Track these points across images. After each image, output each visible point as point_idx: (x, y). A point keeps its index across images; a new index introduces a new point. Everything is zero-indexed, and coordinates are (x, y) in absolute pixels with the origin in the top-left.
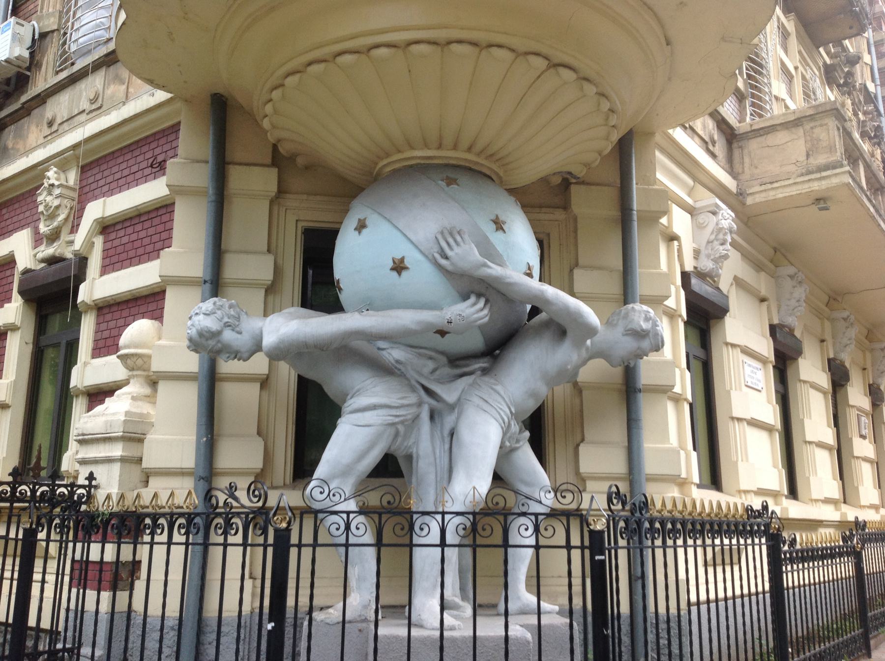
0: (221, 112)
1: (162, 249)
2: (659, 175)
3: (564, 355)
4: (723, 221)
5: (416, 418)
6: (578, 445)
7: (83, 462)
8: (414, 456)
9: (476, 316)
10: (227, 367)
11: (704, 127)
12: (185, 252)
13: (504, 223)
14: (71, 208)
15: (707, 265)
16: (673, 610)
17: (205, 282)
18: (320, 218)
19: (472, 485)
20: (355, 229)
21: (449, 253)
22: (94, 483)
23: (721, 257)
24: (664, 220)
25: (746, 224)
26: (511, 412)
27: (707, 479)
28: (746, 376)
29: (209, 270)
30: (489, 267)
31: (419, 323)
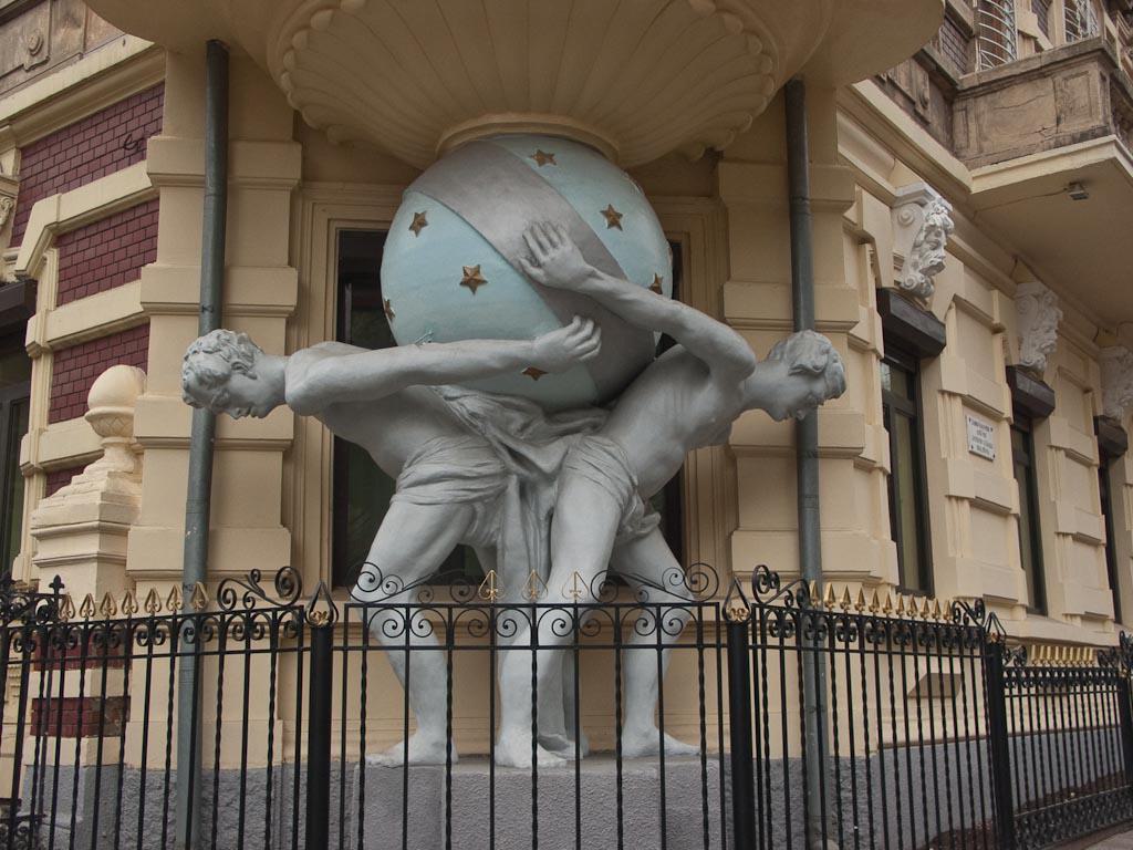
0: (223, 73)
1: (144, 265)
2: (841, 149)
3: (704, 400)
4: (935, 216)
5: (501, 494)
6: (731, 534)
7: (43, 565)
8: (499, 547)
9: (580, 347)
10: (237, 427)
11: (910, 81)
12: (175, 271)
13: (620, 216)
14: (11, 209)
15: (912, 277)
16: (860, 753)
17: (204, 309)
18: (358, 216)
19: (575, 575)
20: (411, 228)
21: (543, 258)
22: (61, 591)
23: (932, 267)
24: (851, 214)
25: (971, 220)
26: (633, 484)
27: (912, 582)
28: (970, 438)
29: (208, 292)
30: (599, 278)
31: (504, 358)
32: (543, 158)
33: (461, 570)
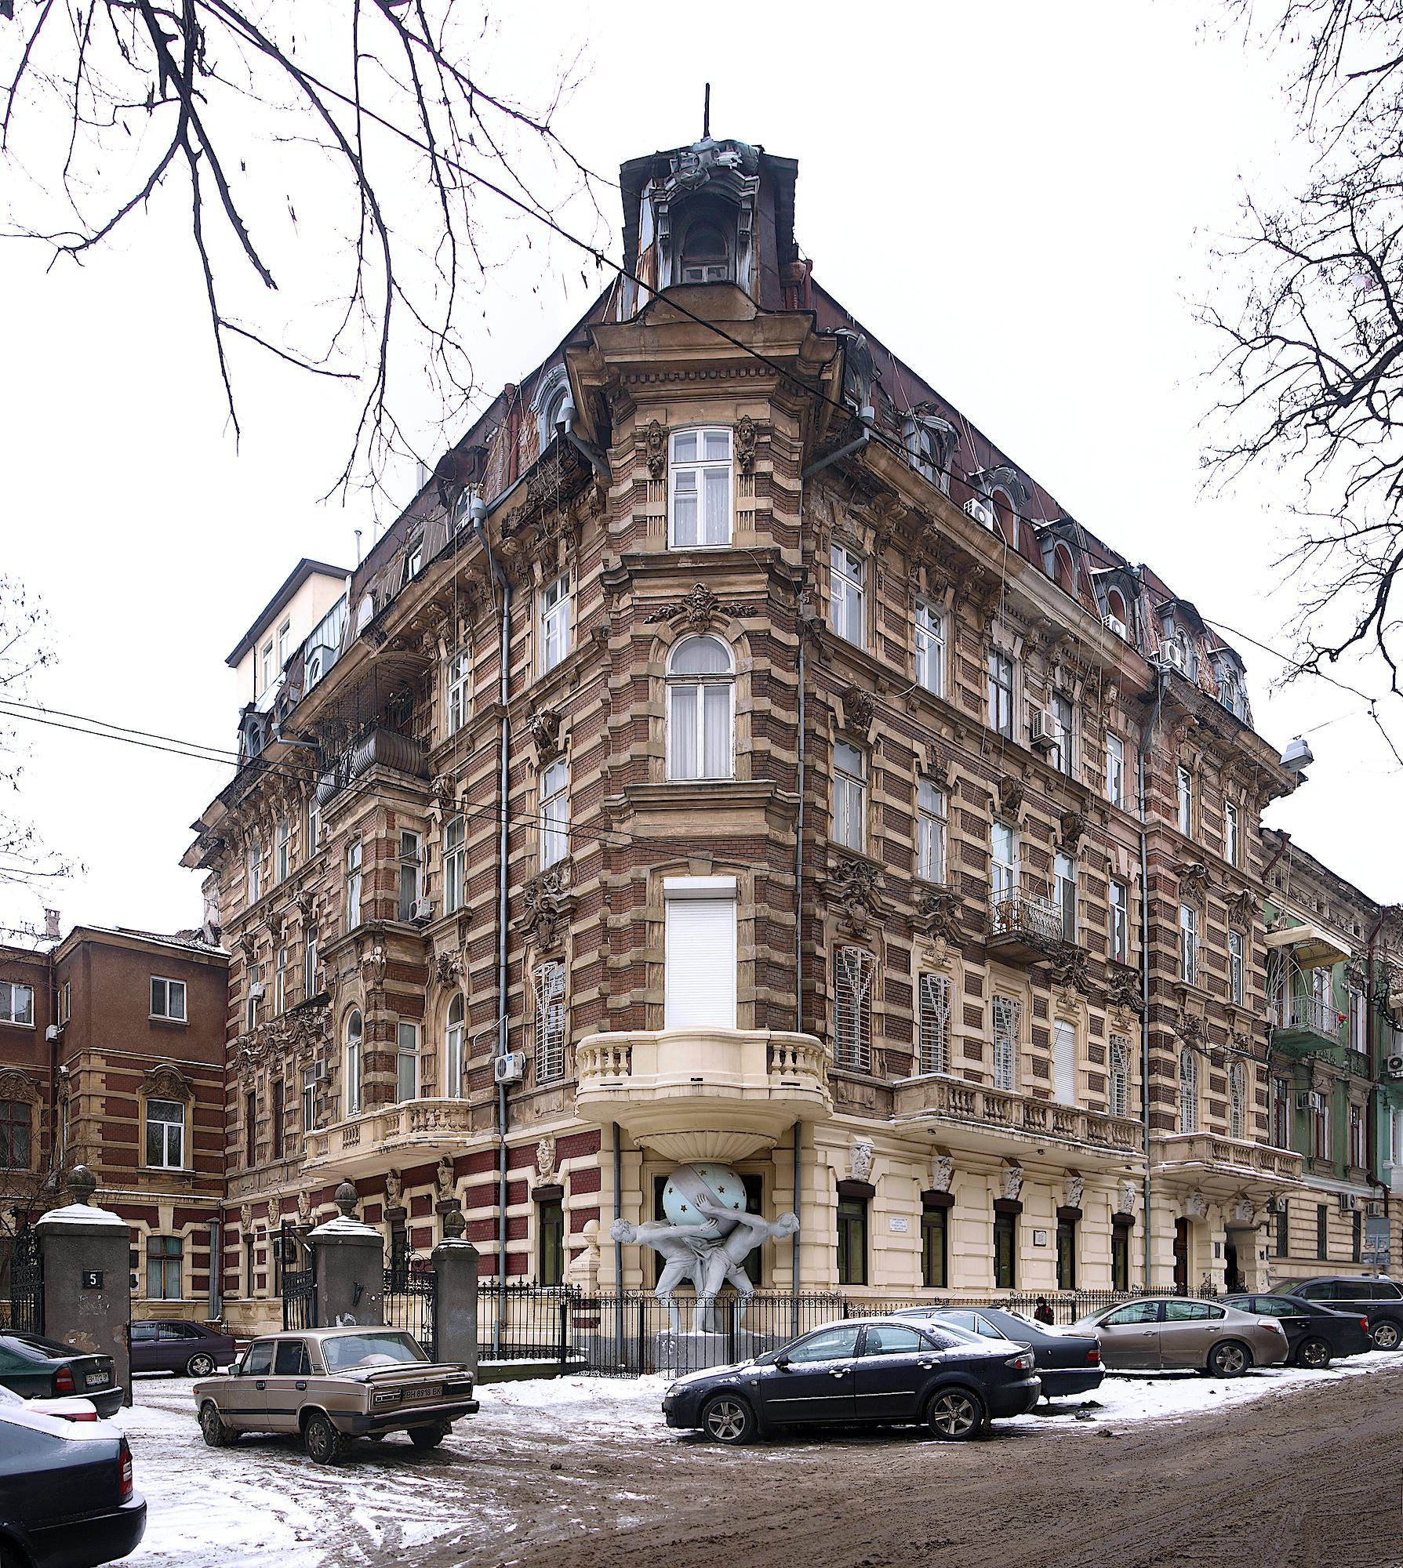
32: (703, 1173)
33: (686, 1283)
